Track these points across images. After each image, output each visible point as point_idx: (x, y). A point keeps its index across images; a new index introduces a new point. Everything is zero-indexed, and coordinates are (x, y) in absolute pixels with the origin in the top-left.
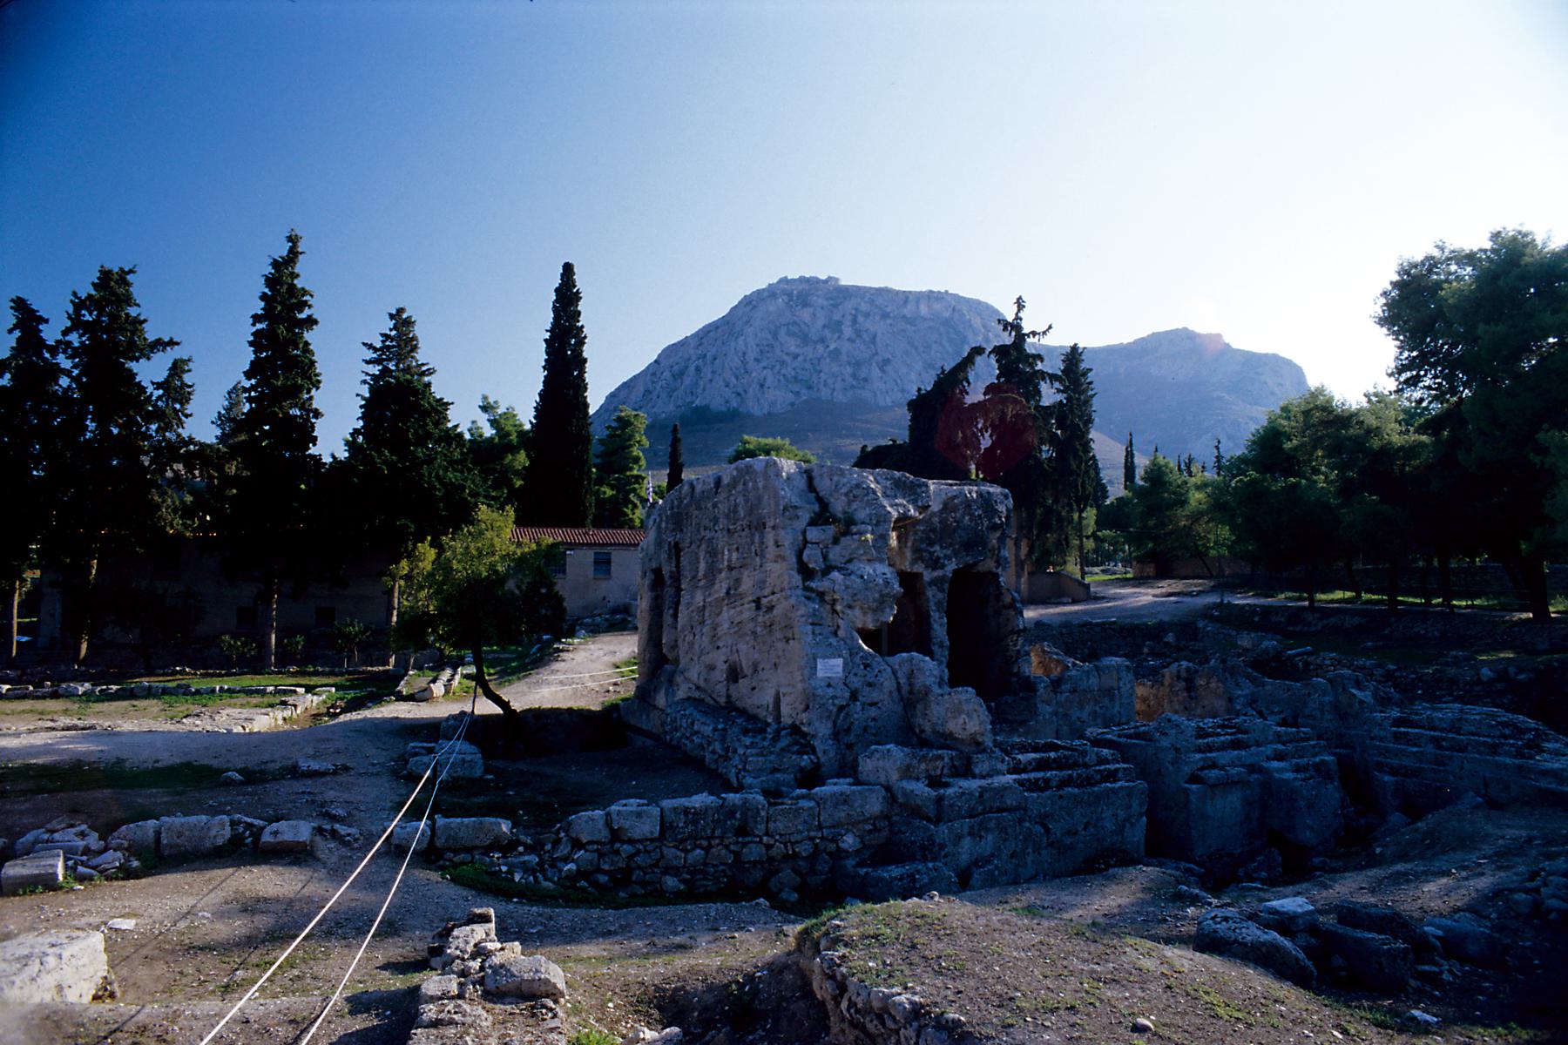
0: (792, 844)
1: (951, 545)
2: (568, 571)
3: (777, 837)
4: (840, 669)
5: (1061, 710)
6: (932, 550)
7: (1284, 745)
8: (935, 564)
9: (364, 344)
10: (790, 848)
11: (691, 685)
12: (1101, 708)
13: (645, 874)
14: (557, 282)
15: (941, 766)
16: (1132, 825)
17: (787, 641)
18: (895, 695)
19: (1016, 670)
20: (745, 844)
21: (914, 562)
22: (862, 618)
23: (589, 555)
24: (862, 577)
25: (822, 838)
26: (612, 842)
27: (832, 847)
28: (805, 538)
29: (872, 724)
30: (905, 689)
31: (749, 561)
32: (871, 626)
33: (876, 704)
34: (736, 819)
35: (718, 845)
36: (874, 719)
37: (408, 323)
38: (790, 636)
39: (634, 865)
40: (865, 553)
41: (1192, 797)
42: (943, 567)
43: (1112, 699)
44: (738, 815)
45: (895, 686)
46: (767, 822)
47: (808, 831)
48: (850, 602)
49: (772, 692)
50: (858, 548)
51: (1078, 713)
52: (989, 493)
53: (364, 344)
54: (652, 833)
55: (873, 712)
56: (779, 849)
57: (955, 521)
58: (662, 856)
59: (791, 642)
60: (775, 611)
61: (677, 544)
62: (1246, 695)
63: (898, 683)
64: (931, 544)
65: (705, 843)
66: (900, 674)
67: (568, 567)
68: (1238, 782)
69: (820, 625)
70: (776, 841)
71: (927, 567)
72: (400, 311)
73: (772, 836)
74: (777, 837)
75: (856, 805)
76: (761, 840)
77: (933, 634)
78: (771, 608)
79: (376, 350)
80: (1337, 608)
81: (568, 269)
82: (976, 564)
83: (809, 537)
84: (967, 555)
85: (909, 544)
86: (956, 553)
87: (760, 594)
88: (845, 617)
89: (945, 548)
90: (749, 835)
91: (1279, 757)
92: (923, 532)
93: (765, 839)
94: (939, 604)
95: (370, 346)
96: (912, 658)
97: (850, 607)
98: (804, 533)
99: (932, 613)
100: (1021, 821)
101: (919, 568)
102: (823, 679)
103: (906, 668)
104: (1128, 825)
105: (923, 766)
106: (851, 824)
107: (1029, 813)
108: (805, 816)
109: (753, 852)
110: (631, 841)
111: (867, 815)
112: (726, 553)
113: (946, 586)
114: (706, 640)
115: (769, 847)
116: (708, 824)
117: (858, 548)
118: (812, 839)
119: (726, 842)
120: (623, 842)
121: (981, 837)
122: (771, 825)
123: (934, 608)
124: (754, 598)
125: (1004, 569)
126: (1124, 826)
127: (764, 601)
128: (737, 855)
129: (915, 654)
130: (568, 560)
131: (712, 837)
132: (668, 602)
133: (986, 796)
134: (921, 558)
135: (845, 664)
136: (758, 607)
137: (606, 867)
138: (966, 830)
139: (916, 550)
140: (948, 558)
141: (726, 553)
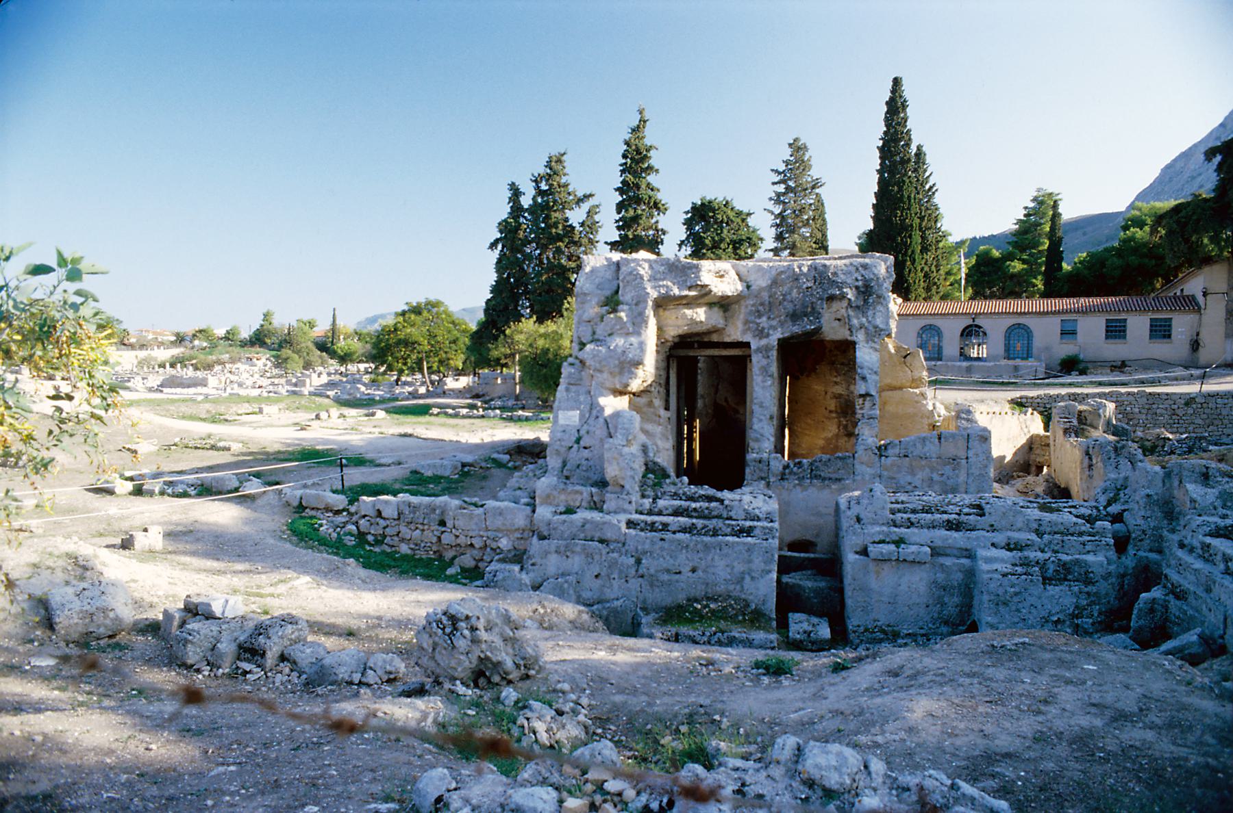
4: (577, 419)
5: (885, 473)
6: (758, 321)
7: (395, 495)
8: (761, 333)
9: (772, 170)
14: (887, 96)
15: (579, 499)
16: (753, 578)
20: (443, 532)
21: (744, 332)
23: (1055, 324)
27: (494, 545)
29: (584, 463)
36: (587, 459)
37: (804, 148)
40: (621, 329)
42: (768, 335)
44: (437, 512)
50: (615, 325)
51: (909, 478)
52: (825, 266)
53: (772, 170)
55: (586, 453)
64: (760, 316)
65: (420, 527)
71: (754, 336)
79: (780, 173)
81: (897, 82)
84: (794, 326)
86: (782, 324)
92: (753, 306)
94: (764, 370)
95: (777, 172)
101: (747, 338)
102: (562, 426)
104: (748, 579)
105: (563, 497)
106: (507, 532)
107: (627, 547)
108: (476, 520)
109: (447, 539)
111: (516, 527)
115: (457, 537)
117: (615, 325)
119: (432, 528)
121: (567, 557)
122: (456, 523)
123: (758, 372)
126: (743, 578)
128: (439, 538)
133: (587, 526)
135: (582, 416)
138: (553, 548)
140: (775, 328)
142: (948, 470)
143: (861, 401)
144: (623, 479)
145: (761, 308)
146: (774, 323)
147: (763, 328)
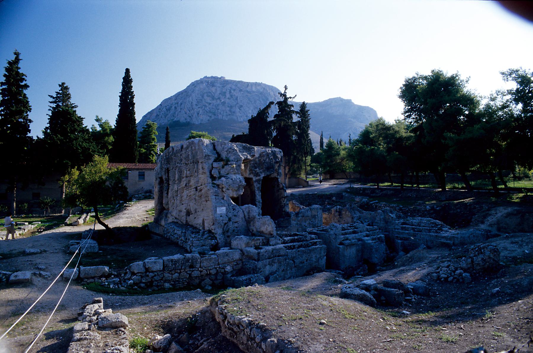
0: (209, 270)
1: (262, 168)
2: (129, 179)
3: (204, 268)
4: (225, 210)
5: (299, 223)
6: (256, 170)
7: (369, 232)
8: (257, 175)
9: (49, 96)
10: (208, 271)
11: (173, 217)
12: (312, 222)
13: (158, 283)
14: (123, 75)
17: (207, 202)
18: (244, 219)
19: (284, 210)
20: (193, 271)
21: (250, 174)
22: (232, 193)
23: (136, 173)
24: (232, 179)
25: (219, 268)
26: (146, 272)
28: (212, 166)
29: (236, 229)
30: (247, 217)
31: (193, 174)
32: (235, 196)
33: (237, 222)
34: (189, 263)
35: (183, 272)
36: (236, 227)
37: (67, 88)
38: (208, 199)
39: (154, 280)
41: (340, 250)
42: (259, 176)
43: (315, 218)
44: (190, 261)
45: (243, 216)
46: (200, 264)
47: (215, 265)
48: (228, 188)
49: (202, 219)
50: (230, 170)
51: (304, 224)
52: (275, 151)
53: (49, 96)
54: (160, 268)
55: (236, 225)
56: (205, 272)
57: (264, 160)
58: (164, 276)
59: (208, 201)
60: (202, 191)
61: (168, 169)
62: (358, 216)
63: (245, 215)
64: (256, 168)
65: (179, 271)
66: (245, 212)
67: (129, 177)
68: (354, 244)
69: (218, 196)
70: (204, 269)
71: (254, 176)
72: (63, 84)
73: (202, 268)
74: (204, 268)
75: (231, 256)
76: (198, 270)
77: (256, 198)
78: (201, 190)
79: (54, 98)
80: (386, 188)
81: (127, 71)
82: (270, 175)
83: (214, 166)
84: (268, 172)
85: (248, 168)
86: (264, 171)
87: (197, 185)
88: (226, 193)
89: (260, 169)
90: (194, 268)
91: (367, 236)
92: (253, 164)
93: (200, 269)
94: (258, 188)
95: (51, 97)
96: (249, 206)
97: (228, 189)
98: (212, 164)
99: (256, 191)
100: (286, 259)
101: (251, 176)
102: (219, 214)
103: (247, 210)
104: (320, 259)
105: (253, 243)
106: (229, 263)
107: (288, 257)
108: (213, 261)
109: (196, 273)
110: (153, 272)
111: (234, 259)
112: (185, 171)
113: (261, 182)
114: (178, 201)
115: (201, 271)
116: (180, 265)
117: (230, 170)
118: (216, 268)
119: (186, 270)
120: (150, 272)
121: (272, 265)
122: (202, 264)
123: (257, 189)
124: (195, 187)
125: (280, 176)
126: (319, 260)
127: (198, 188)
128: (190, 274)
129: (250, 205)
130: (129, 174)
131: (181, 269)
132: (165, 188)
133: (274, 251)
134: (252, 173)
135: (227, 209)
136: (196, 190)
137: (144, 281)
138: (268, 263)
139: (251, 170)
140: (261, 173)
141: (185, 171)
142: (313, 220)
143: (284, 199)
144: (273, 231)
145: (256, 165)
146: (261, 171)
147: (258, 173)
